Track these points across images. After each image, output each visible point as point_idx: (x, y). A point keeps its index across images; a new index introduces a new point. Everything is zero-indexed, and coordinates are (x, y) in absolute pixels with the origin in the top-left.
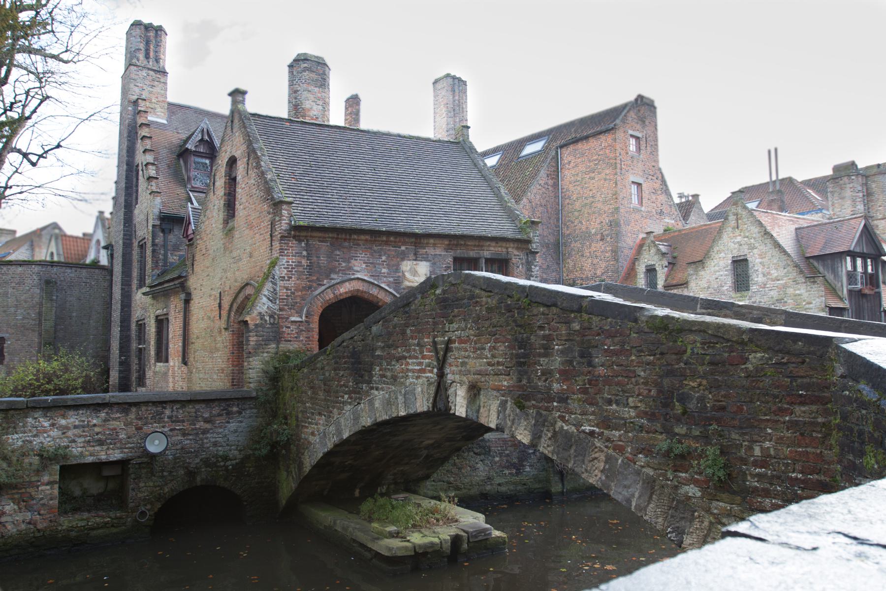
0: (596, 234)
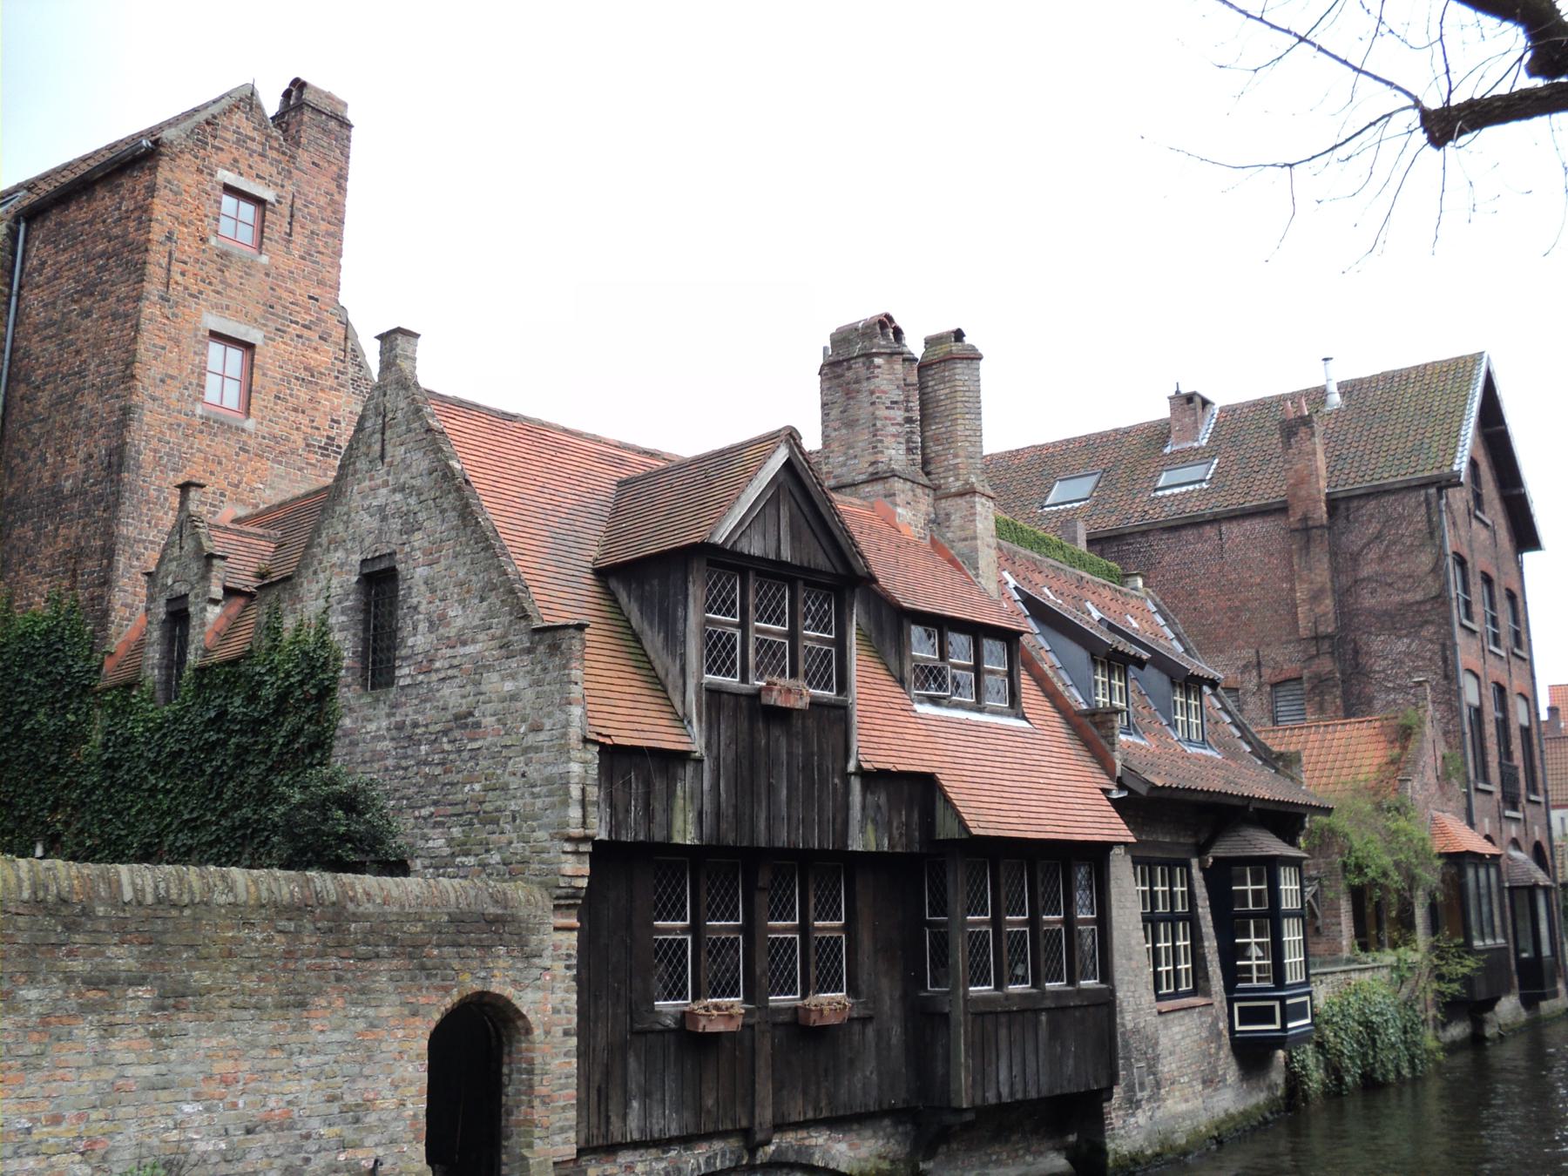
0: (74, 495)
